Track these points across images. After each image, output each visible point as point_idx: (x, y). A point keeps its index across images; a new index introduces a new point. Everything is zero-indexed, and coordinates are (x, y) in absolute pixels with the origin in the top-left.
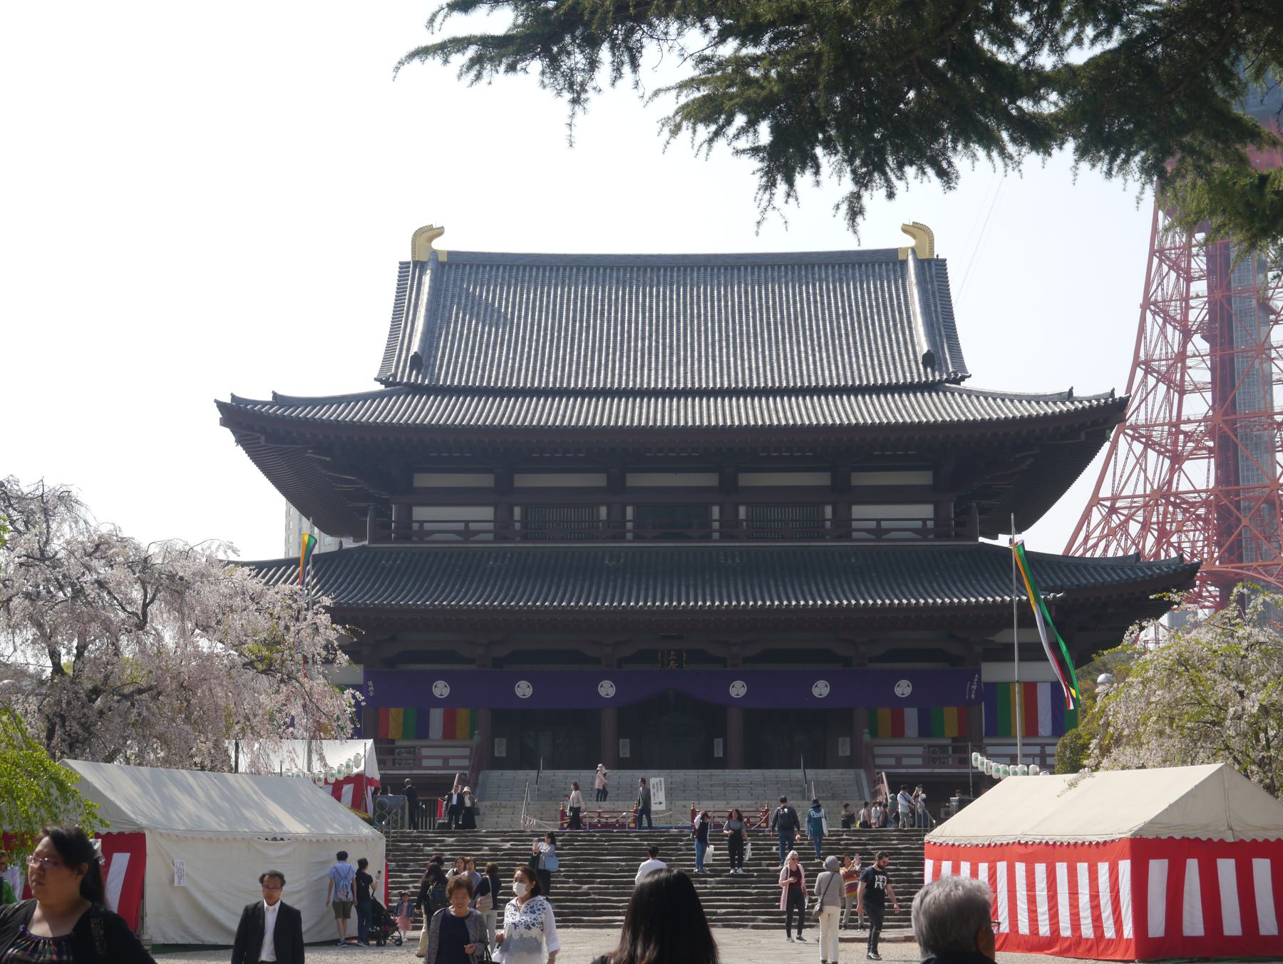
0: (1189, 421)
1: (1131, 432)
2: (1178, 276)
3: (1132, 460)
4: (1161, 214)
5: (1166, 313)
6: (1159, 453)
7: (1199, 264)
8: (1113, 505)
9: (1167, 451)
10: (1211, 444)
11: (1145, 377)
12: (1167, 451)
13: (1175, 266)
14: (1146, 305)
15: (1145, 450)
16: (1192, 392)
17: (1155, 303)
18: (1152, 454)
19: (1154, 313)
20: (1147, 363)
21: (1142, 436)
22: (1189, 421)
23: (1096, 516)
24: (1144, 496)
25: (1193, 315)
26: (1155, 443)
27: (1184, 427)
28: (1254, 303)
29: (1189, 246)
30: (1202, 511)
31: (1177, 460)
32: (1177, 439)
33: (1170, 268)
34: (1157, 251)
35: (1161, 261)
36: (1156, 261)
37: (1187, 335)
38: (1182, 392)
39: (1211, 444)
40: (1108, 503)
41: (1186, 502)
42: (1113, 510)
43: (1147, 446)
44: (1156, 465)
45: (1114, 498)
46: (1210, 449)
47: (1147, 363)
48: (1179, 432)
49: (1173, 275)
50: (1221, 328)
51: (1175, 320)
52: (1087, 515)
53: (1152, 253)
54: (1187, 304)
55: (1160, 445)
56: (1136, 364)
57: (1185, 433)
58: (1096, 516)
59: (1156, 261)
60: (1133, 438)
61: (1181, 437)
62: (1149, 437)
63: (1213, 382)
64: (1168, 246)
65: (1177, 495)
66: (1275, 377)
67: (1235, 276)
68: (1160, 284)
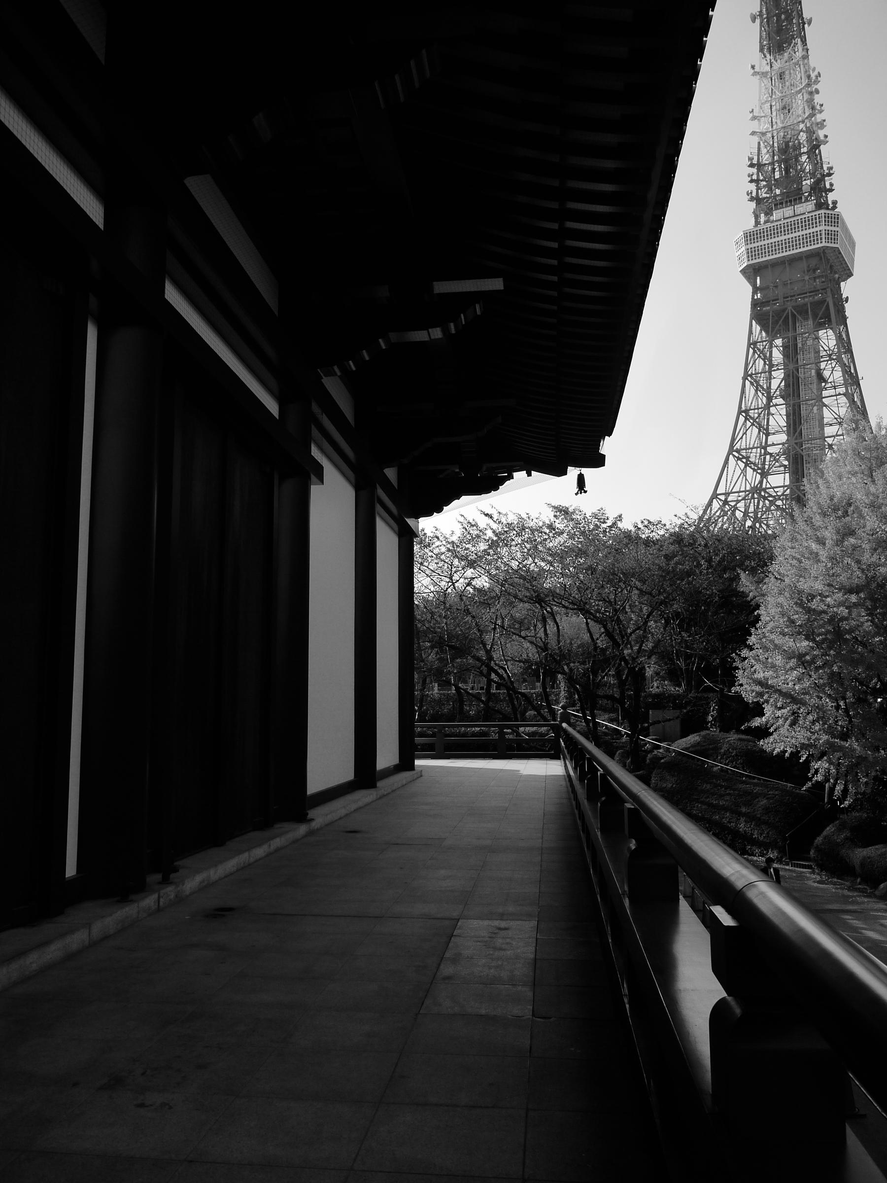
0: (773, 444)
1: (737, 455)
3: (738, 472)
4: (754, 322)
5: (757, 382)
6: (754, 470)
7: (777, 356)
8: (726, 499)
9: (759, 469)
10: (786, 463)
11: (745, 421)
12: (759, 469)
14: (745, 379)
15: (745, 467)
16: (774, 434)
18: (749, 471)
19: (752, 383)
20: (746, 411)
21: (744, 457)
22: (773, 444)
23: (716, 505)
24: (745, 491)
25: (775, 384)
26: (752, 463)
27: (769, 449)
28: (813, 372)
30: (779, 503)
31: (764, 474)
32: (765, 458)
34: (752, 344)
35: (754, 352)
37: (770, 399)
38: (768, 434)
39: (786, 463)
40: (723, 498)
41: (771, 496)
42: (726, 502)
43: (746, 465)
44: (753, 477)
45: (727, 494)
46: (785, 466)
47: (746, 411)
48: (766, 453)
50: (793, 389)
51: (763, 388)
52: (710, 504)
54: (771, 375)
55: (755, 464)
56: (740, 412)
57: (771, 454)
58: (716, 505)
59: (751, 351)
60: (739, 459)
61: (768, 457)
62: (748, 458)
63: (788, 426)
65: (765, 490)
66: (826, 421)
67: (800, 357)
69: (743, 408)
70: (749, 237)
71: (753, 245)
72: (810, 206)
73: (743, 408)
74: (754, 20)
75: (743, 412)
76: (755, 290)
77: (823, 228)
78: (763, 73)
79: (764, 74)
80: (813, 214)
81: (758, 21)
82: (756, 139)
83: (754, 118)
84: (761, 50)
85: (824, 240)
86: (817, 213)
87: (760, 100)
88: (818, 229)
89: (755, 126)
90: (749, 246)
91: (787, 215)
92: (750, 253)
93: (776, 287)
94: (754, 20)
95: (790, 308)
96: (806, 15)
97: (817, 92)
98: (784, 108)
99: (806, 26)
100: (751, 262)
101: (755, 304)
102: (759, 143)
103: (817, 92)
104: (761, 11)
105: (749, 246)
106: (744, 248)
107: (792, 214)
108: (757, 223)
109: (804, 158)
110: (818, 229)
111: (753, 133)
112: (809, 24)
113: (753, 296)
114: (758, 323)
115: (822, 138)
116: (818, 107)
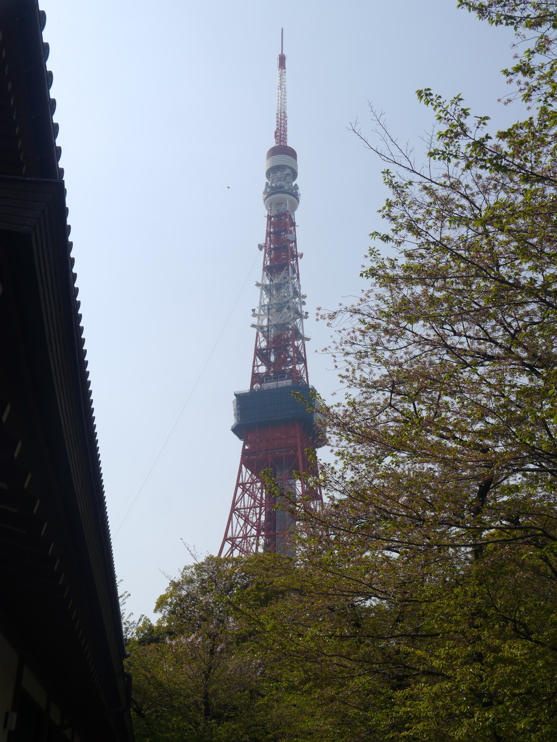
4: (244, 468)
17: (237, 509)
56: (226, 539)
59: (240, 490)
69: (229, 534)
73: (229, 534)
74: (261, 250)
75: (230, 539)
81: (263, 250)
82: (255, 330)
83: (254, 315)
87: (260, 303)
89: (255, 321)
94: (260, 248)
96: (299, 251)
97: (304, 303)
99: (299, 258)
102: (257, 335)
103: (304, 303)
104: (266, 244)
111: (253, 326)
112: (301, 258)
113: (244, 447)
114: (247, 467)
116: (304, 314)
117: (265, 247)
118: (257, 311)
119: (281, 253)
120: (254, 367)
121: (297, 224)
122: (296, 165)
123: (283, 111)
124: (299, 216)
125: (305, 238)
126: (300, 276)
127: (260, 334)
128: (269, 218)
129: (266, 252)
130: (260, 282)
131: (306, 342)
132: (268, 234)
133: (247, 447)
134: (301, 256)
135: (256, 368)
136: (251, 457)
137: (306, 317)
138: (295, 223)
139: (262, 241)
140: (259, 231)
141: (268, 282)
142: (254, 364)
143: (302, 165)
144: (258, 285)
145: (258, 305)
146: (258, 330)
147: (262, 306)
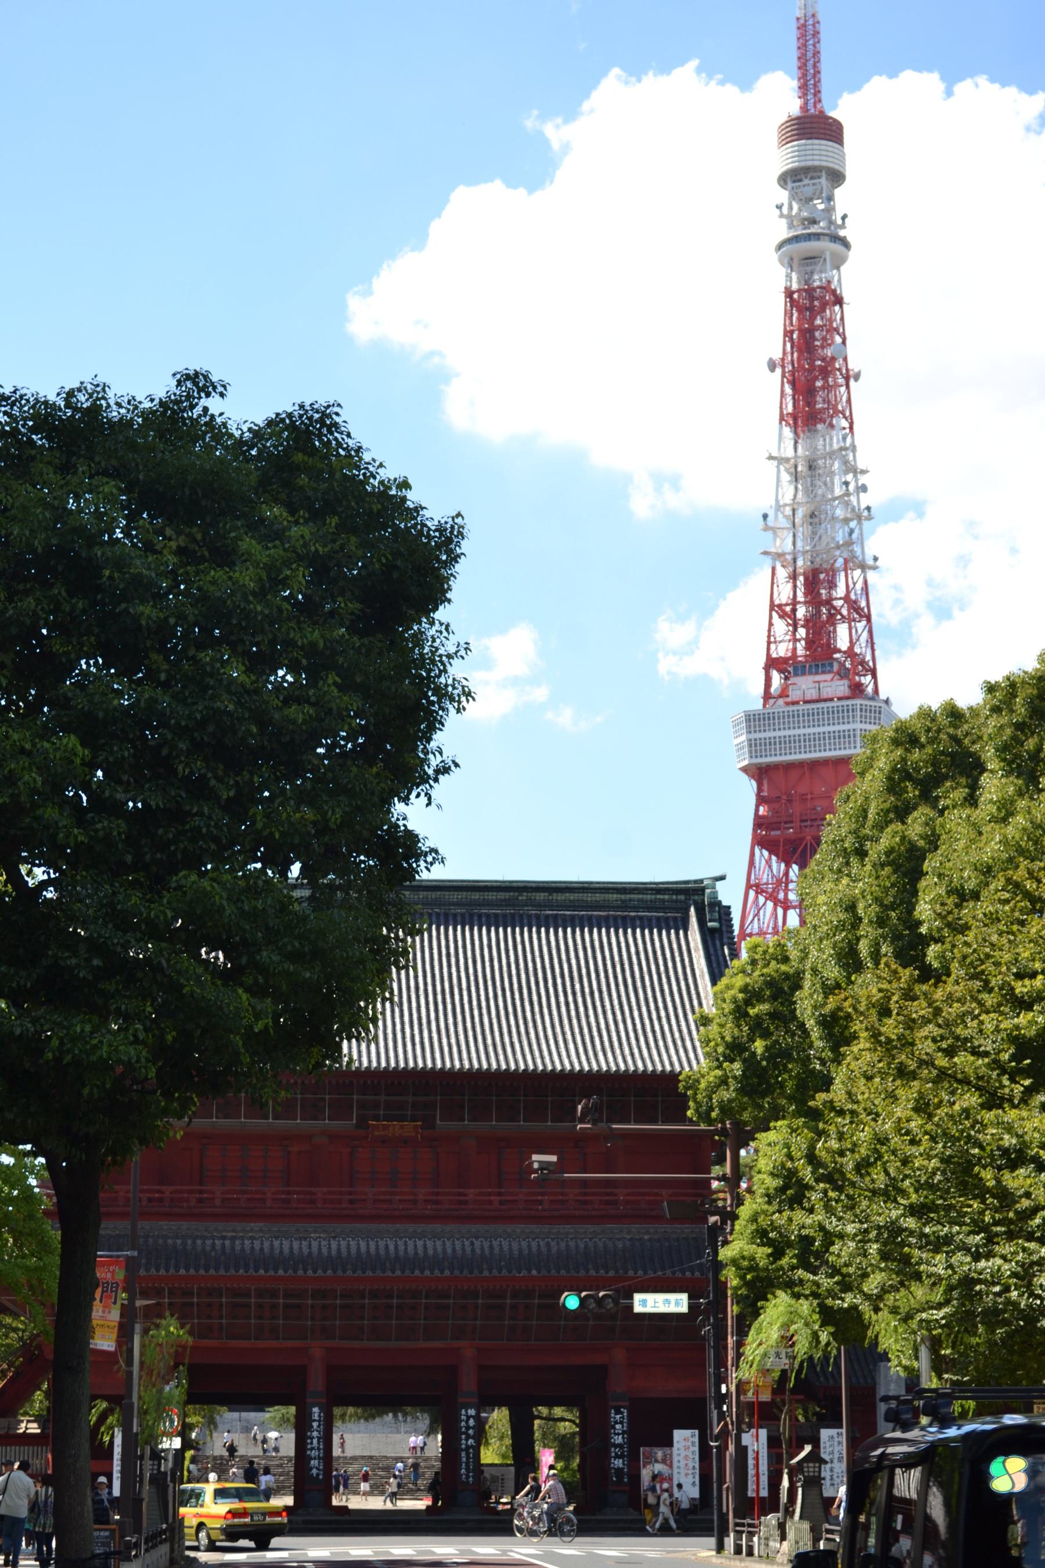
2: (775, 905)
13: (772, 897)
29: (786, 874)
33: (767, 899)
36: (752, 893)
49: (770, 905)
53: (749, 886)
59: (752, 893)
64: (765, 881)
68: (757, 915)
70: (753, 721)
71: (758, 735)
72: (841, 687)
76: (761, 800)
77: (858, 726)
78: (782, 459)
79: (781, 460)
80: (845, 703)
81: (779, 371)
83: (767, 528)
84: (782, 418)
85: (858, 745)
86: (850, 702)
87: (777, 501)
88: (851, 726)
90: (753, 736)
91: (808, 697)
92: (753, 746)
93: (790, 801)
95: (809, 838)
96: (853, 365)
98: (812, 515)
99: (852, 382)
100: (755, 761)
101: (759, 823)
102: (774, 569)
103: (864, 488)
104: (783, 359)
105: (753, 736)
106: (744, 738)
107: (815, 696)
108: (767, 696)
109: (840, 603)
110: (851, 726)
113: (757, 810)
115: (871, 562)
117: (783, 367)
118: (770, 520)
119: (813, 379)
120: (769, 643)
121: (846, 300)
122: (843, 155)
123: (809, 14)
124: (851, 279)
125: (865, 335)
126: (855, 427)
127: (778, 565)
128: (789, 293)
129: (783, 376)
130: (775, 454)
131: (871, 575)
132: (788, 334)
133: (762, 810)
134: (857, 377)
135: (773, 646)
136: (773, 833)
137: (869, 518)
138: (842, 298)
139: (777, 355)
140: (768, 332)
141: (790, 453)
142: (769, 636)
143: (856, 153)
144: (771, 458)
145: (773, 503)
146: (774, 560)
147: (779, 507)
